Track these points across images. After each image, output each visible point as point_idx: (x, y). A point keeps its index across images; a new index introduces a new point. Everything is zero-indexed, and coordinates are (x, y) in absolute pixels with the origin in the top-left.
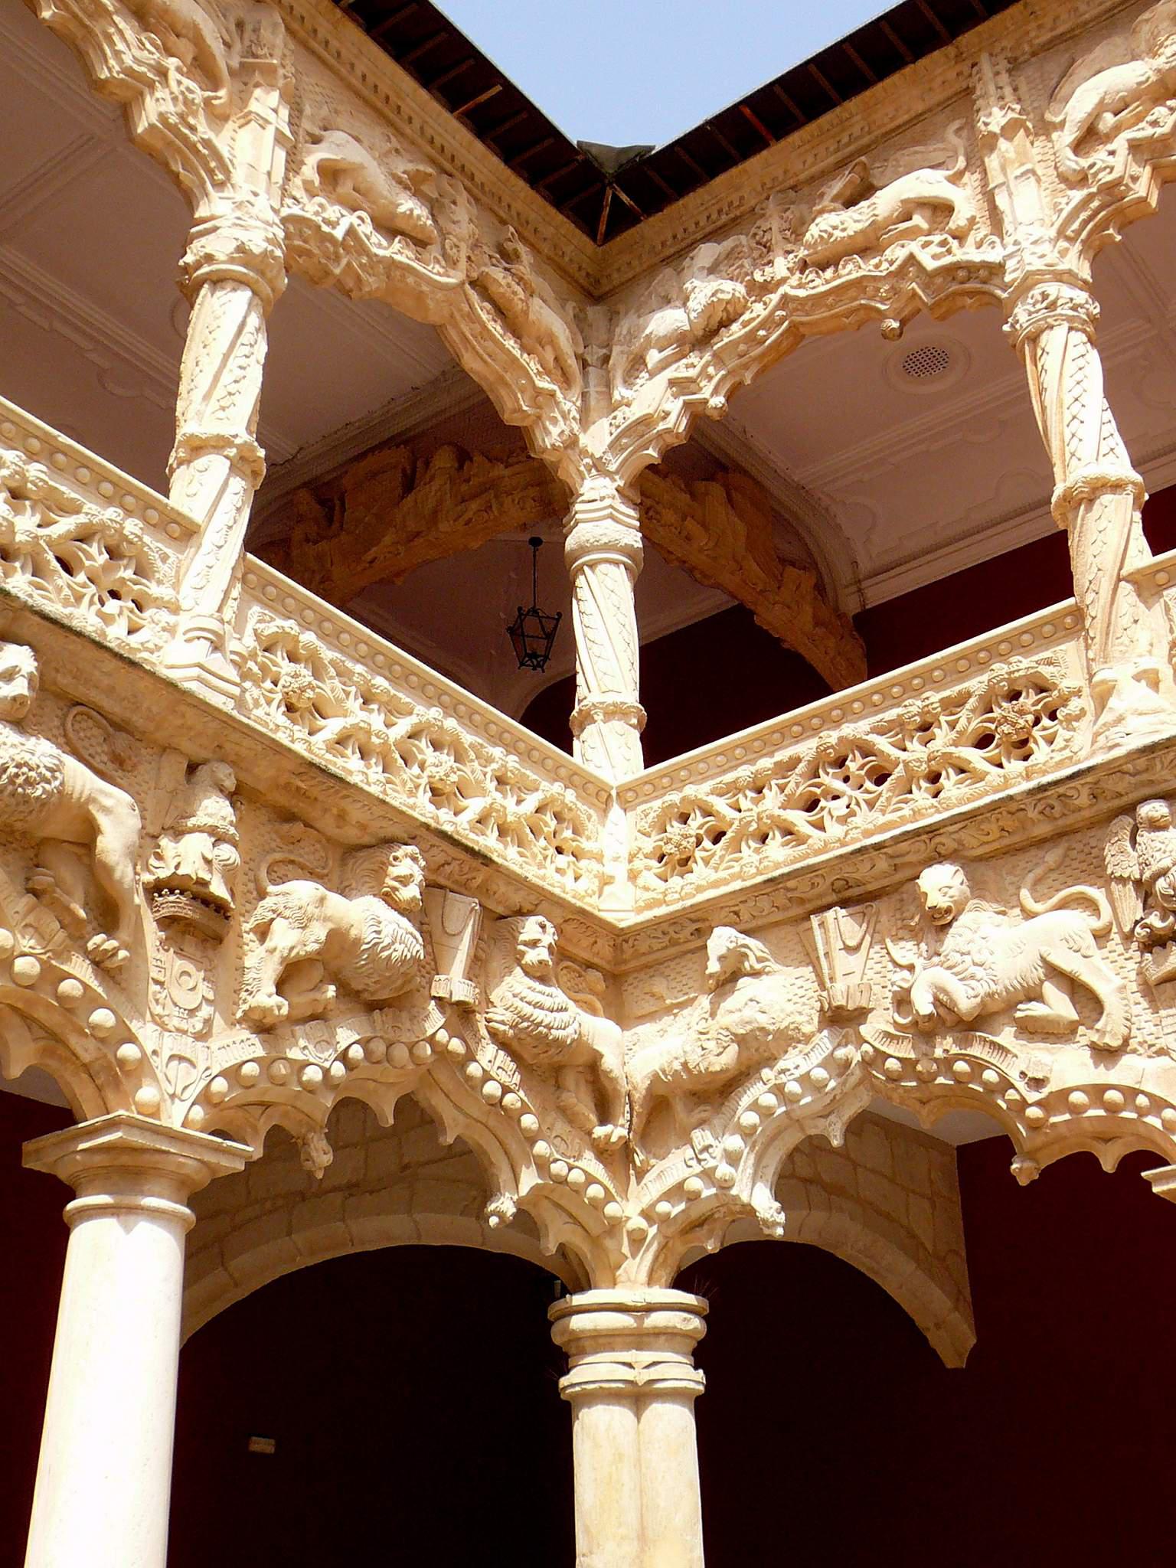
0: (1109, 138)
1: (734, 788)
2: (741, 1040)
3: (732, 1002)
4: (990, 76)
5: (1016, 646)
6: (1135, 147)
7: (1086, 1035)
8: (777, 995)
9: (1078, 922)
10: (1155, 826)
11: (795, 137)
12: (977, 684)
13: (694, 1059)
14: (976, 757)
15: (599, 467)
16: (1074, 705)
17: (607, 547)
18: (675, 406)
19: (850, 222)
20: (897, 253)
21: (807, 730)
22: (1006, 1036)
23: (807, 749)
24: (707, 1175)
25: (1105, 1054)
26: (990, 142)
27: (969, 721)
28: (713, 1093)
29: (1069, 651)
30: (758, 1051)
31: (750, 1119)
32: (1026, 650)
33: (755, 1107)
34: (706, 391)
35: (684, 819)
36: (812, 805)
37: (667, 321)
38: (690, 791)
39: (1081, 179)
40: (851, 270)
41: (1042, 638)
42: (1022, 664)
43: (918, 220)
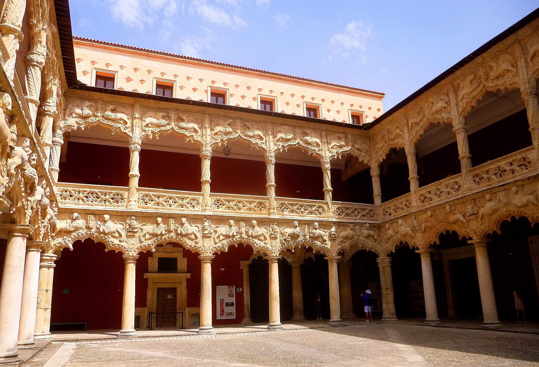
0: (149, 127)
1: (76, 190)
2: (75, 227)
3: (74, 222)
4: (137, 106)
5: (120, 189)
6: (152, 131)
7: (119, 239)
8: (81, 223)
9: (121, 226)
10: (133, 219)
11: (107, 95)
12: (114, 192)
13: (68, 228)
14: (111, 200)
15: (61, 129)
16: (125, 200)
17: (59, 143)
18: (76, 126)
19: (113, 115)
20: (119, 125)
21: (89, 187)
22: (110, 236)
23: (88, 190)
24: (65, 242)
25: (120, 241)
26: (135, 118)
27: (111, 196)
28: (68, 232)
29: (126, 193)
30: (77, 229)
31: (73, 237)
32: (121, 190)
33: (74, 235)
34: (82, 126)
35: (66, 191)
36: (87, 197)
37: (78, 111)
38: (68, 188)
39: (144, 131)
40: (110, 123)
41: (123, 190)
42: (121, 192)
43: (122, 121)
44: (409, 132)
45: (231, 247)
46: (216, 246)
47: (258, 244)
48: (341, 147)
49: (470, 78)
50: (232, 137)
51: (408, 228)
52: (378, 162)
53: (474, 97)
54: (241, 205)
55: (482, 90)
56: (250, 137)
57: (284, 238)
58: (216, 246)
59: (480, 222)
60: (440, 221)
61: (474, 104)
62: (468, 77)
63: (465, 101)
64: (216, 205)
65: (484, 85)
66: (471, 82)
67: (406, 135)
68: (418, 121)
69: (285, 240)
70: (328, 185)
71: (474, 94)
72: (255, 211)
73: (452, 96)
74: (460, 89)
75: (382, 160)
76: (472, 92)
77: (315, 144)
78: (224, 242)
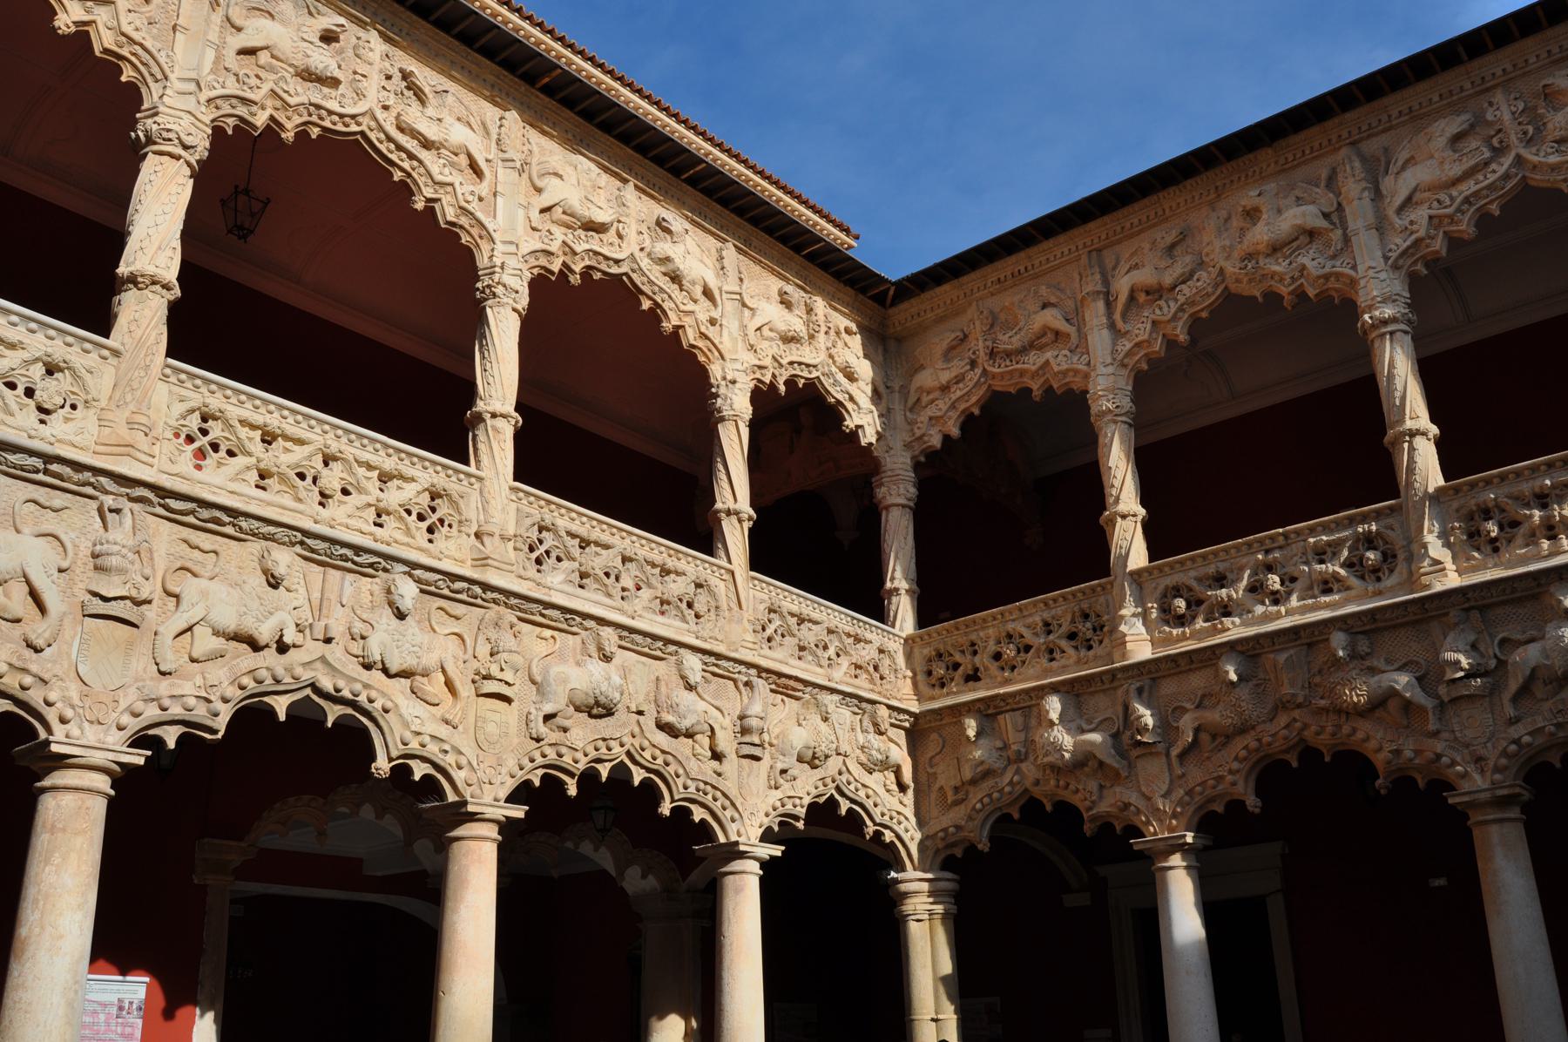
44: (1112, 326)
45: (252, 716)
46: (164, 688)
47: (407, 728)
48: (789, 339)
49: (1453, 125)
50: (333, 105)
51: (1096, 737)
52: (918, 448)
53: (1467, 200)
54: (333, 478)
55: (1506, 177)
56: (427, 144)
57: (549, 708)
58: (164, 688)
59: (1510, 711)
60: (1282, 705)
61: (1465, 226)
62: (1441, 124)
63: (1421, 215)
64: (190, 439)
65: (1519, 161)
66: (1457, 138)
67: (1100, 339)
68: (1168, 280)
69: (548, 718)
70: (734, 490)
71: (1469, 187)
72: (408, 532)
73: (1353, 187)
74: (1393, 169)
75: (936, 441)
76: (1456, 182)
77: (698, 291)
78: (219, 674)
